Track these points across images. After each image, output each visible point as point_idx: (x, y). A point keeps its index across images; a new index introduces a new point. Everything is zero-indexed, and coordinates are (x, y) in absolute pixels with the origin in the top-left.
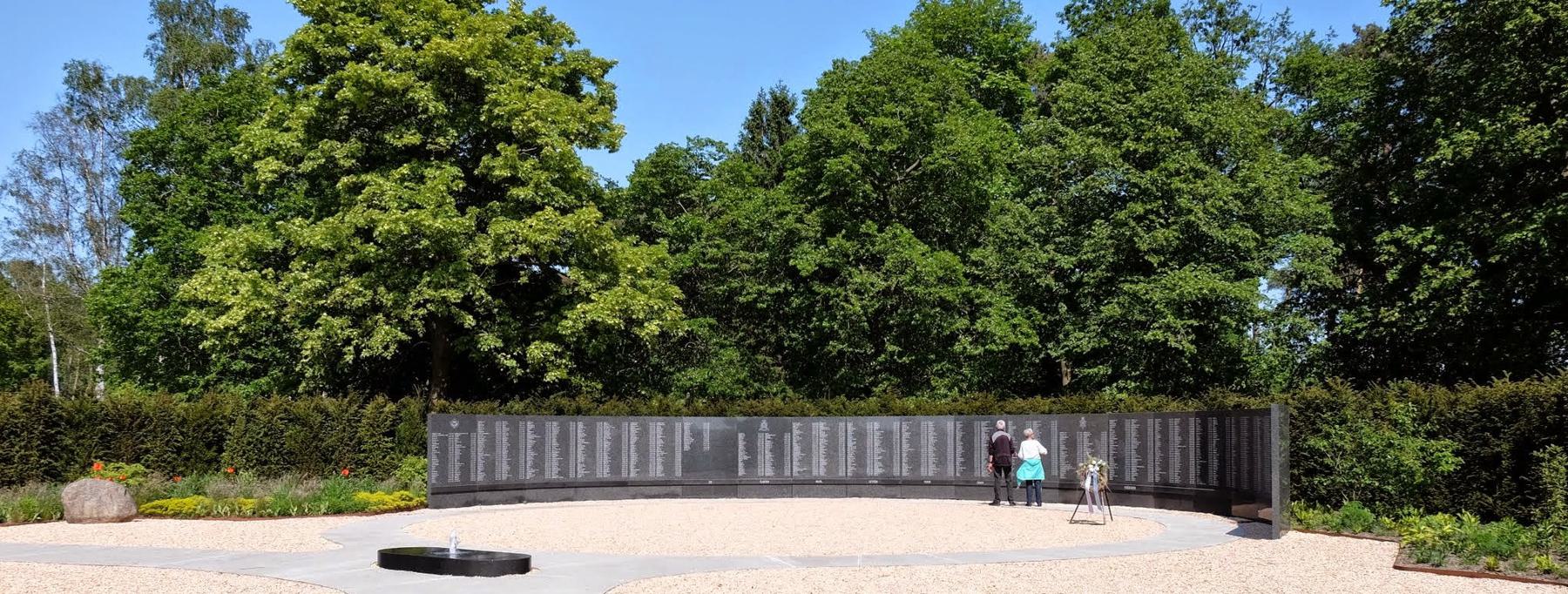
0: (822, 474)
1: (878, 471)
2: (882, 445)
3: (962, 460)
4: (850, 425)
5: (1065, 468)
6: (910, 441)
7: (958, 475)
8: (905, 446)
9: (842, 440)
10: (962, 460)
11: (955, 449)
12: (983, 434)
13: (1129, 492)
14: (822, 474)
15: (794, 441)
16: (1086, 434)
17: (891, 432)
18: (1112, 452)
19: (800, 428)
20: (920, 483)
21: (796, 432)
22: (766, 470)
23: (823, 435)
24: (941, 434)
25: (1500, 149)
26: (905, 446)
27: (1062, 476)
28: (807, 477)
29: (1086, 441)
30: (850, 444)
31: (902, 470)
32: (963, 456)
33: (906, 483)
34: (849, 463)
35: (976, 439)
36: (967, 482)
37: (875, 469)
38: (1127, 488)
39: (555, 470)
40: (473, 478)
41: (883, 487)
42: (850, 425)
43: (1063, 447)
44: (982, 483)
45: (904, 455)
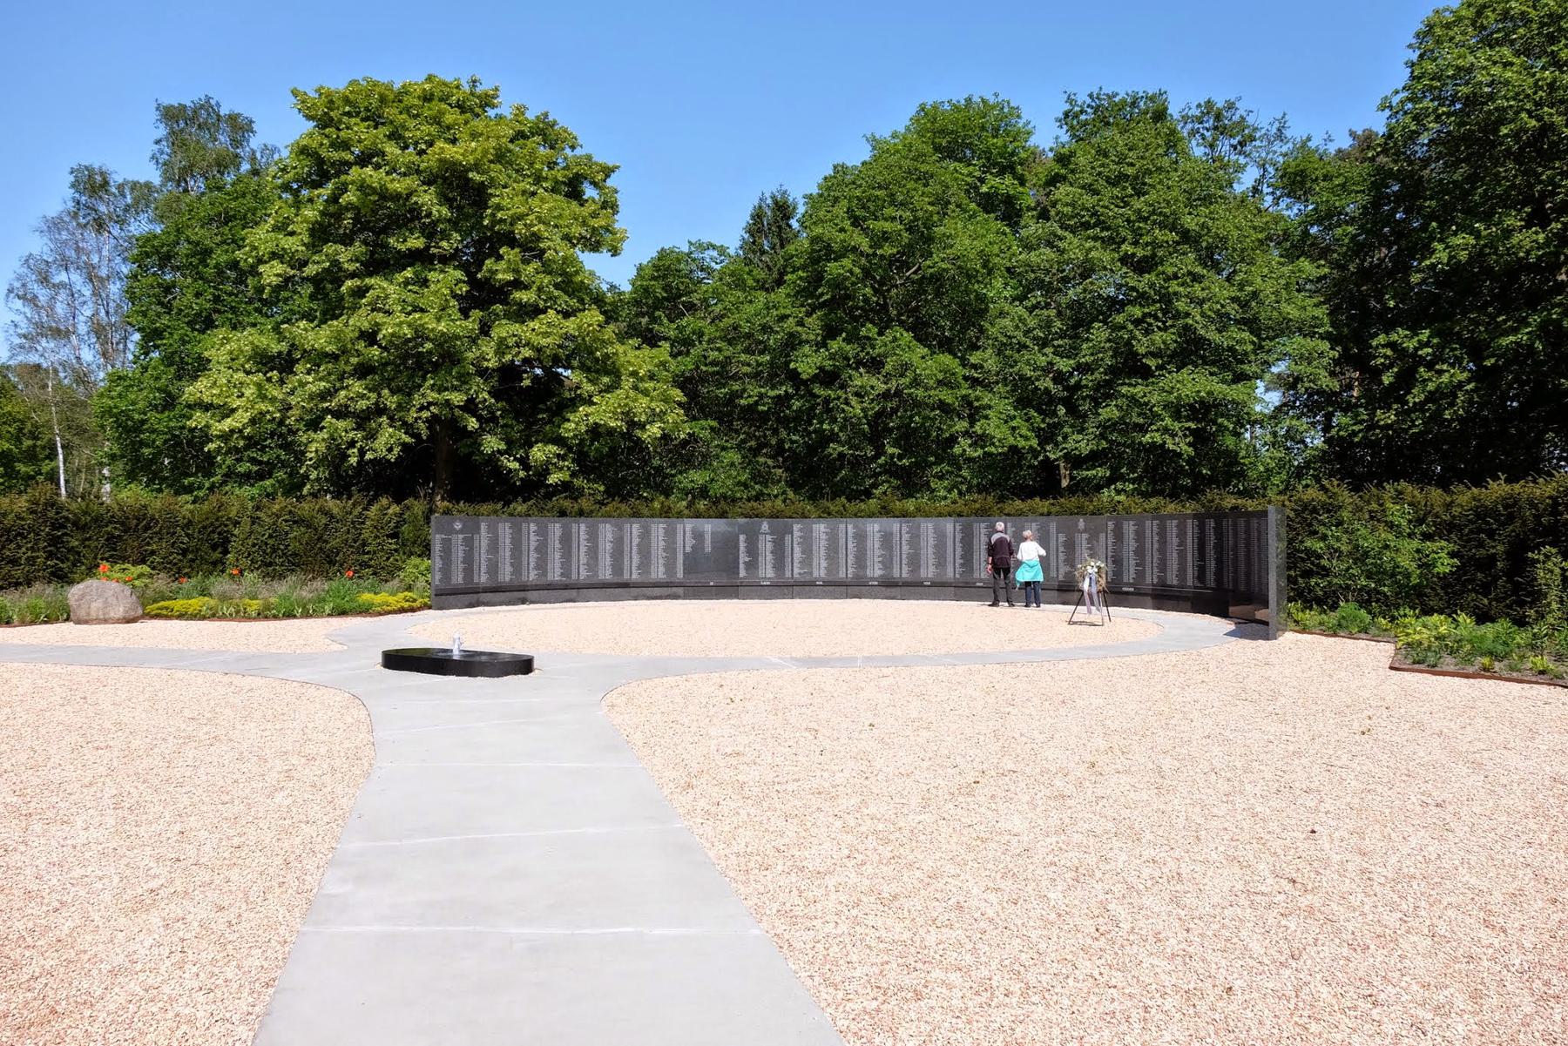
0: (822, 575)
1: (878, 573)
4: (850, 527)
5: (1063, 569)
6: (910, 543)
8: (905, 548)
11: (954, 551)
13: (1127, 593)
14: (822, 575)
16: (1085, 536)
17: (891, 534)
18: (1110, 554)
19: (801, 530)
20: (919, 584)
21: (797, 534)
22: (767, 571)
23: (824, 537)
24: (941, 536)
25: (1495, 253)
26: (905, 548)
28: (808, 578)
29: (1084, 543)
30: (850, 545)
31: (902, 572)
32: (962, 557)
33: (906, 584)
35: (975, 541)
37: (875, 571)
38: (1125, 589)
39: (558, 571)
42: (850, 527)
43: (1061, 549)
45: (904, 557)
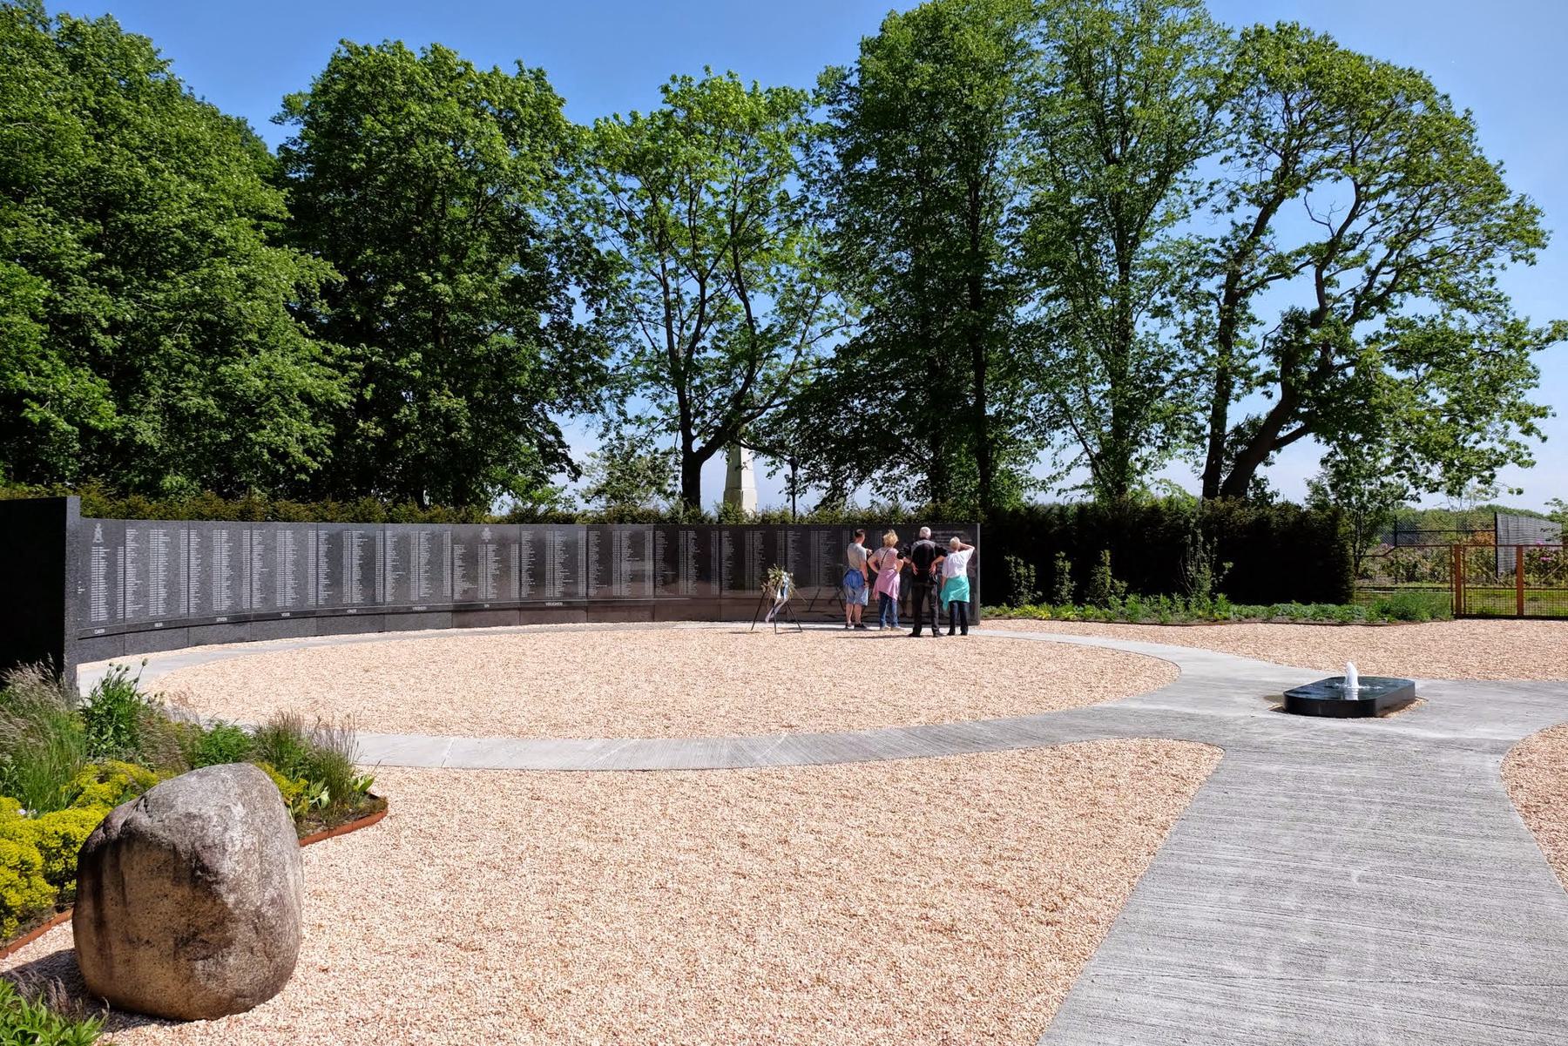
0: (161, 612)
1: (225, 605)
2: (231, 567)
3: (327, 582)
4: (193, 534)
5: (461, 586)
6: (263, 557)
7: (321, 602)
8: (257, 564)
9: (184, 555)
10: (327, 582)
11: (316, 567)
12: (355, 546)
13: (552, 608)
14: (161, 612)
15: (128, 561)
16: (491, 547)
17: (576, 543)
18: (525, 567)
19: (136, 539)
20: (277, 617)
21: (130, 545)
22: (420, 590)
23: (162, 549)
24: (301, 546)
25: (588, 345)
26: (257, 564)
27: (457, 597)
28: (144, 619)
29: (491, 555)
30: (193, 562)
31: (254, 602)
32: (328, 576)
33: (261, 618)
34: (192, 591)
35: (346, 553)
36: (334, 611)
37: (222, 603)
38: (548, 604)
39: (290, 593)
40: (379, 599)
41: (231, 627)
42: (388, 533)
43: (458, 562)
44: (354, 611)
45: (256, 577)
